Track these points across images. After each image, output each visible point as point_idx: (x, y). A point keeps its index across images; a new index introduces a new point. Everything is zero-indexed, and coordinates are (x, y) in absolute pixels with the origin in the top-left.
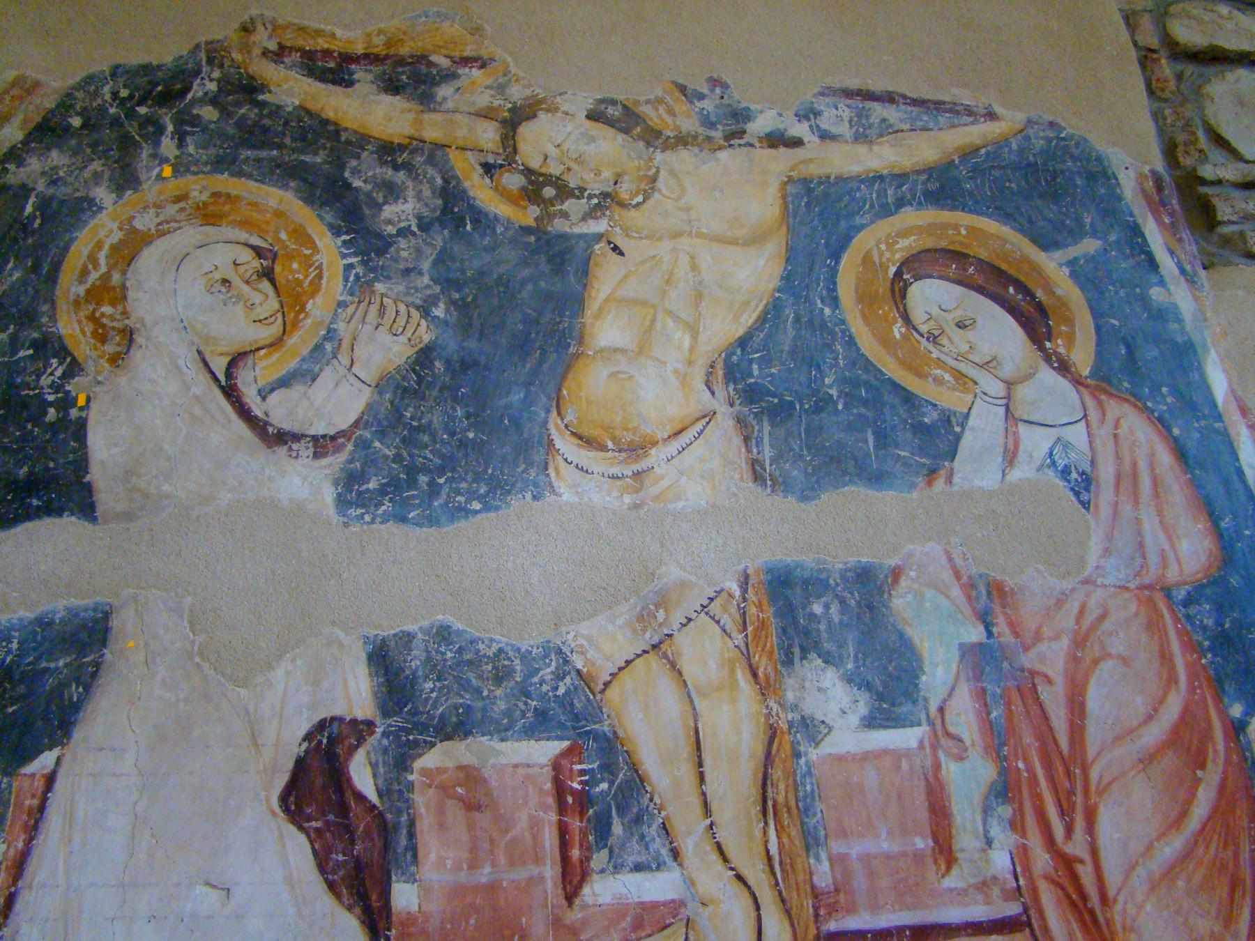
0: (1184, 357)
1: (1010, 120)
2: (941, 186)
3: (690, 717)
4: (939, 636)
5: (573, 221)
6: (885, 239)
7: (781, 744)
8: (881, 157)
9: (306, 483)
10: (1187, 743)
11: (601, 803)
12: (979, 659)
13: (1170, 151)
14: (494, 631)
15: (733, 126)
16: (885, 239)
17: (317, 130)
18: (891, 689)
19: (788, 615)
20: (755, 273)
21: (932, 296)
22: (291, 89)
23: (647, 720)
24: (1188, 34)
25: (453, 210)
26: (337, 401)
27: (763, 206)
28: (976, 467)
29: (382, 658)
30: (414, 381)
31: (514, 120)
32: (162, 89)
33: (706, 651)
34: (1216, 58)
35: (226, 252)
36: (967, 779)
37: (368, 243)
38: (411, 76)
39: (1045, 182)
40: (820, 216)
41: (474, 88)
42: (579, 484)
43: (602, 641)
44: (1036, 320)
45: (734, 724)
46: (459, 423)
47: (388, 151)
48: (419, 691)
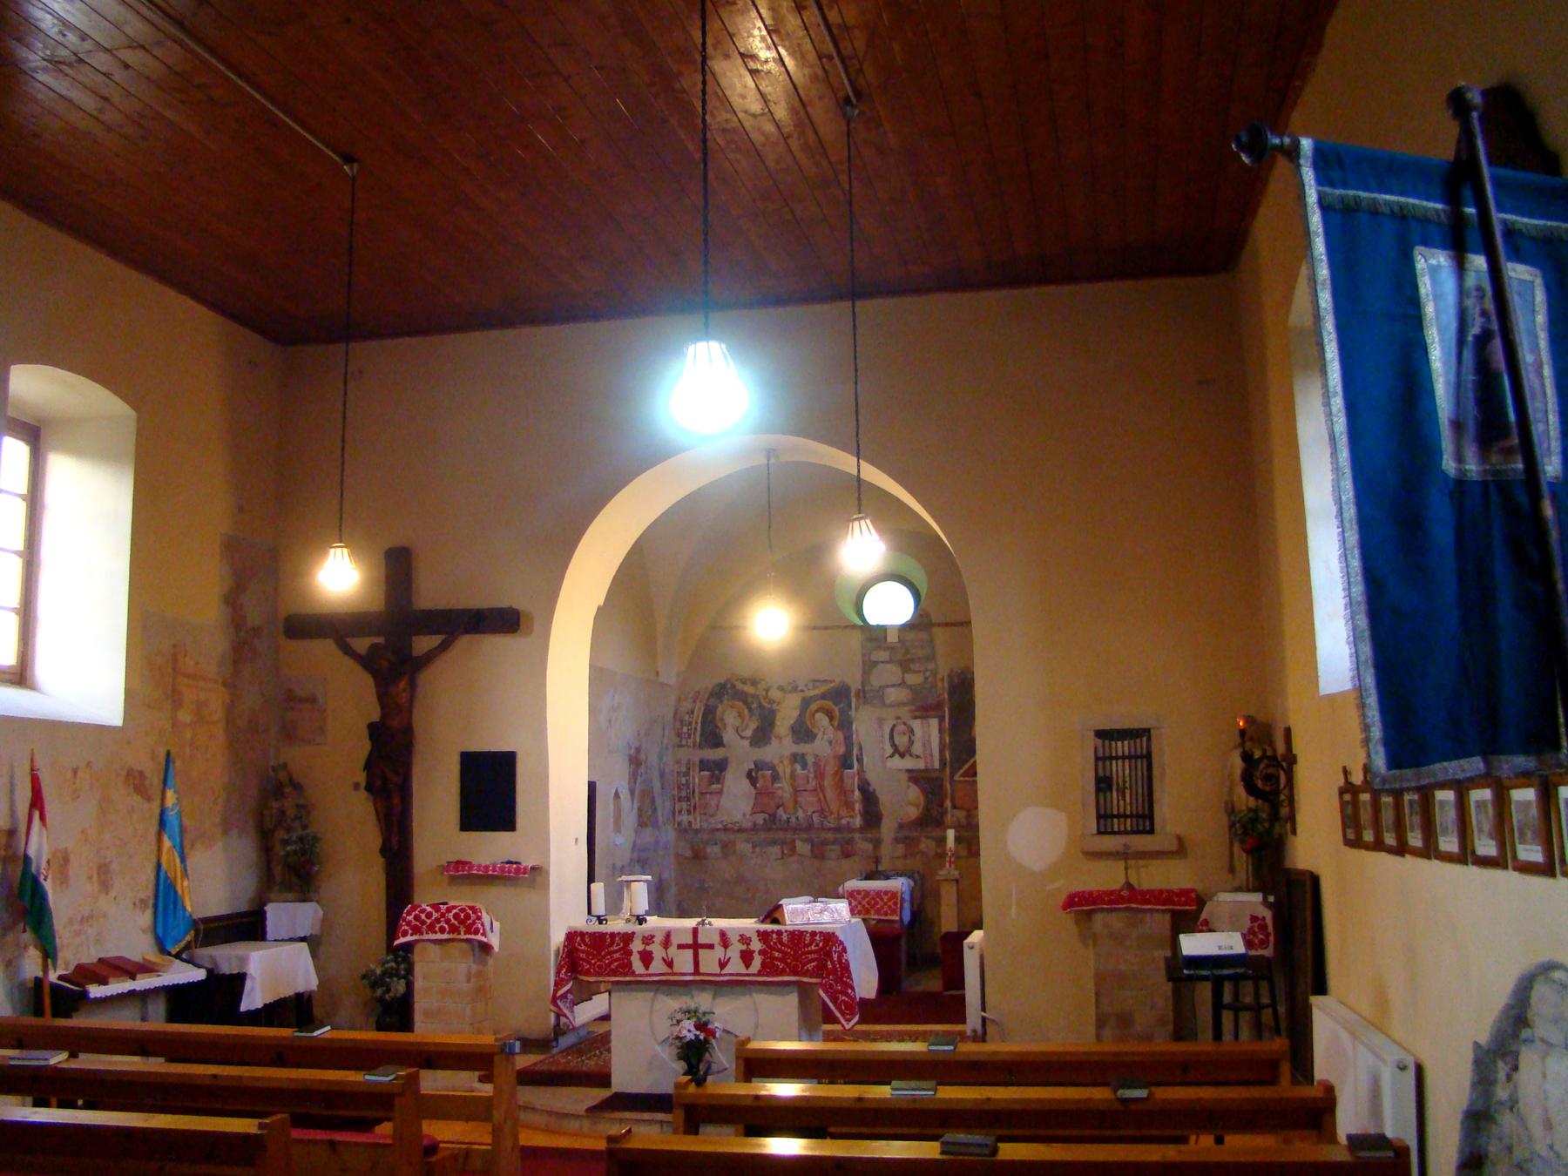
0: (851, 724)
1: (838, 680)
2: (823, 696)
3: (784, 769)
4: (810, 760)
5: (775, 707)
6: (814, 706)
7: (793, 775)
8: (812, 693)
9: (747, 743)
10: (836, 773)
11: (775, 777)
12: (815, 764)
13: (863, 684)
14: (768, 759)
15: (795, 689)
16: (814, 706)
17: (743, 692)
18: (804, 766)
19: (796, 758)
20: (796, 713)
21: (819, 716)
22: (739, 686)
23: (780, 769)
24: (873, 658)
25: (761, 706)
26: (749, 733)
27: (798, 703)
28: (817, 742)
29: (756, 764)
30: (756, 731)
31: (767, 690)
32: (723, 686)
33: (786, 762)
34: (876, 663)
35: (735, 713)
36: (812, 776)
37: (750, 710)
38: (754, 683)
39: (840, 694)
40: (806, 703)
41: (762, 686)
42: (774, 743)
43: (776, 762)
44: (831, 718)
45: (788, 770)
46: (763, 735)
47: (753, 696)
48: (759, 766)
